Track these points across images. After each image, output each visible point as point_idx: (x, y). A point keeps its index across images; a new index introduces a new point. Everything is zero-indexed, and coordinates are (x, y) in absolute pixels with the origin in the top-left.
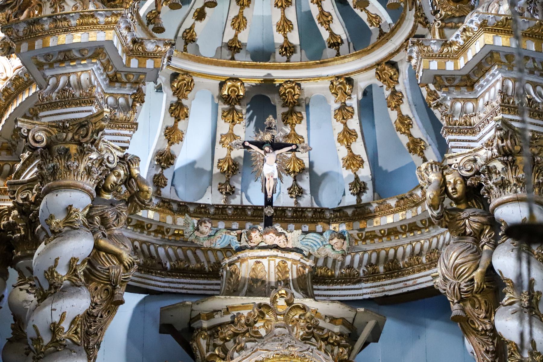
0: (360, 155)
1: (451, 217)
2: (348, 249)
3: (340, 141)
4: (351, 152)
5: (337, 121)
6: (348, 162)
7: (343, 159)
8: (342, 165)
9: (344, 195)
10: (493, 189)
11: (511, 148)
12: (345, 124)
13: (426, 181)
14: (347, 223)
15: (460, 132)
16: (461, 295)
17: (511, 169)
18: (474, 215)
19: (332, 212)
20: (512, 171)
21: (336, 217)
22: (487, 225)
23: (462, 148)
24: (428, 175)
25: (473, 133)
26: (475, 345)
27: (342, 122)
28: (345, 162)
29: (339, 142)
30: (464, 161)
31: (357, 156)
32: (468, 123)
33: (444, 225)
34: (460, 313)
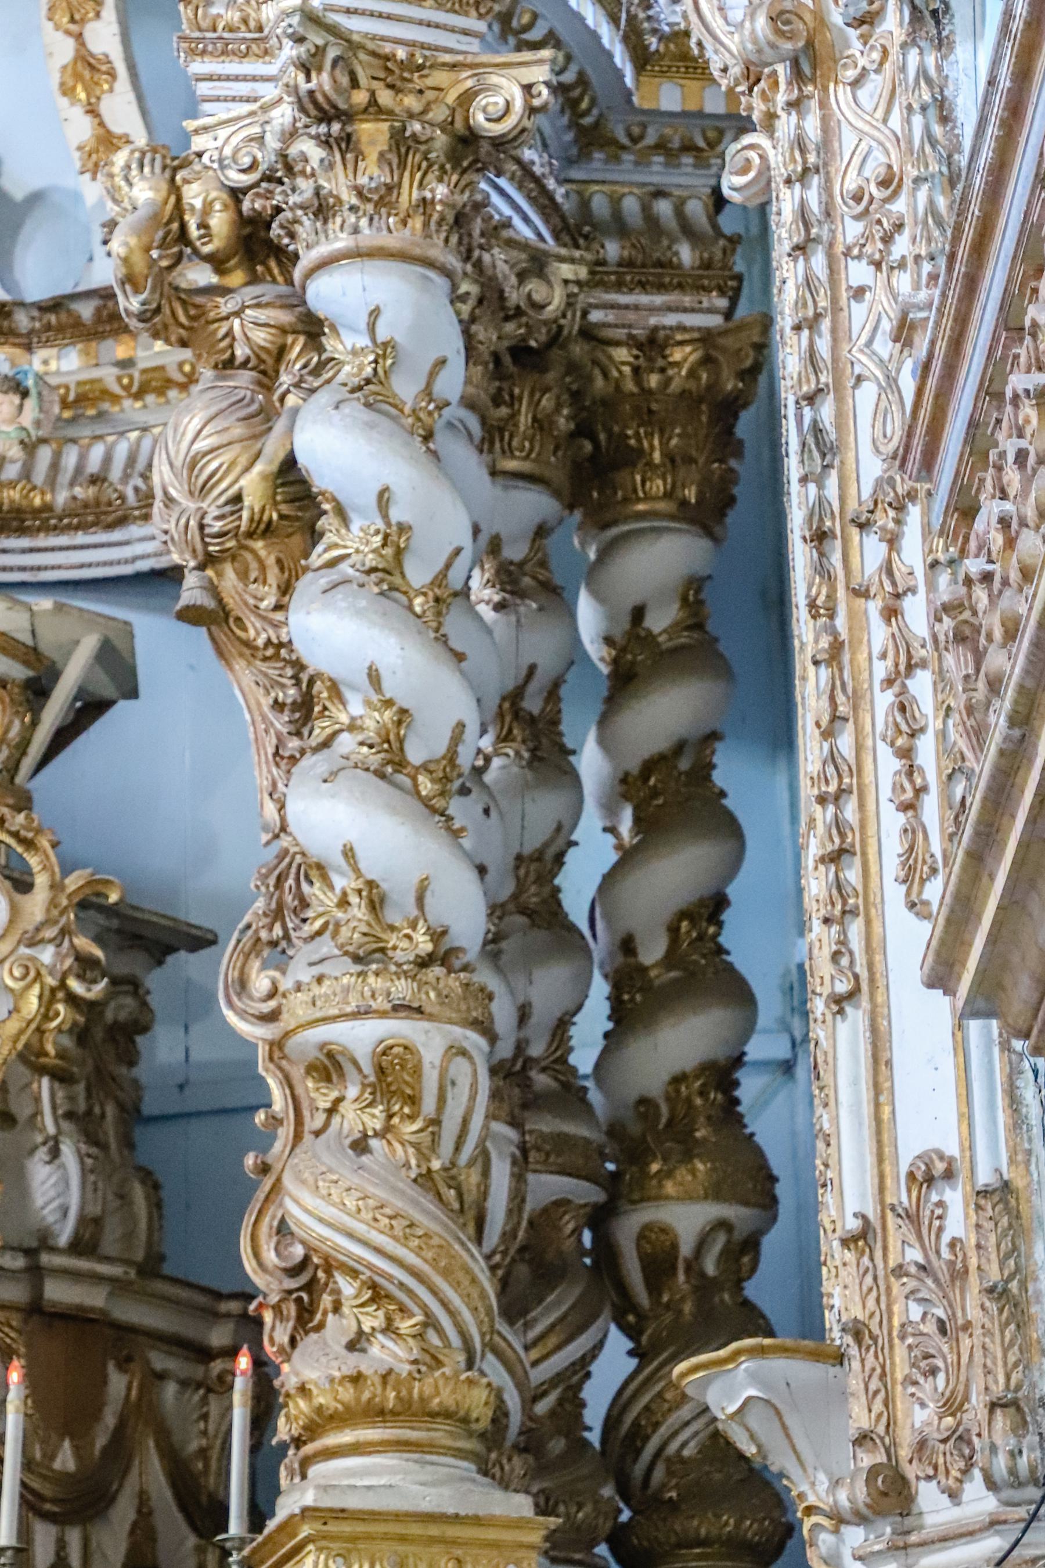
0: (127, 135)
1: (192, 312)
2: (38, 424)
3: (67, 91)
4: (102, 124)
5: (57, 28)
6: (94, 157)
7: (80, 148)
8: (78, 165)
9: (91, 259)
10: (301, 223)
11: (334, 96)
12: (79, 37)
13: (126, 204)
14: (80, 346)
15: (224, 53)
16: (206, 545)
17: (343, 159)
18: (258, 306)
19: (35, 313)
20: (345, 165)
21: (48, 327)
22: (294, 332)
23: (234, 99)
24: (130, 184)
25: (266, 52)
26: (246, 689)
27: (68, 33)
28: (86, 156)
29: (64, 93)
30: (235, 141)
31: (120, 138)
32: (252, 24)
33: (173, 338)
34: (209, 603)
